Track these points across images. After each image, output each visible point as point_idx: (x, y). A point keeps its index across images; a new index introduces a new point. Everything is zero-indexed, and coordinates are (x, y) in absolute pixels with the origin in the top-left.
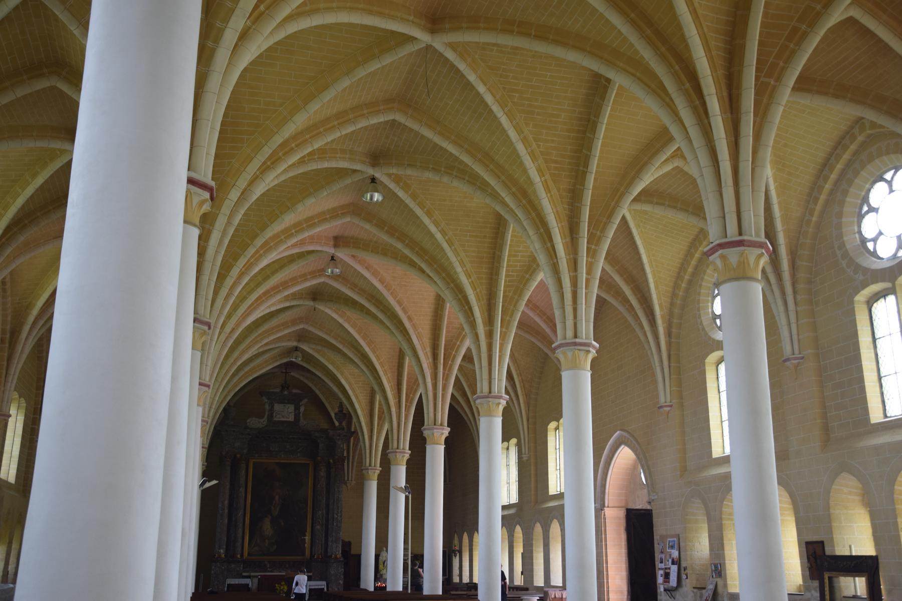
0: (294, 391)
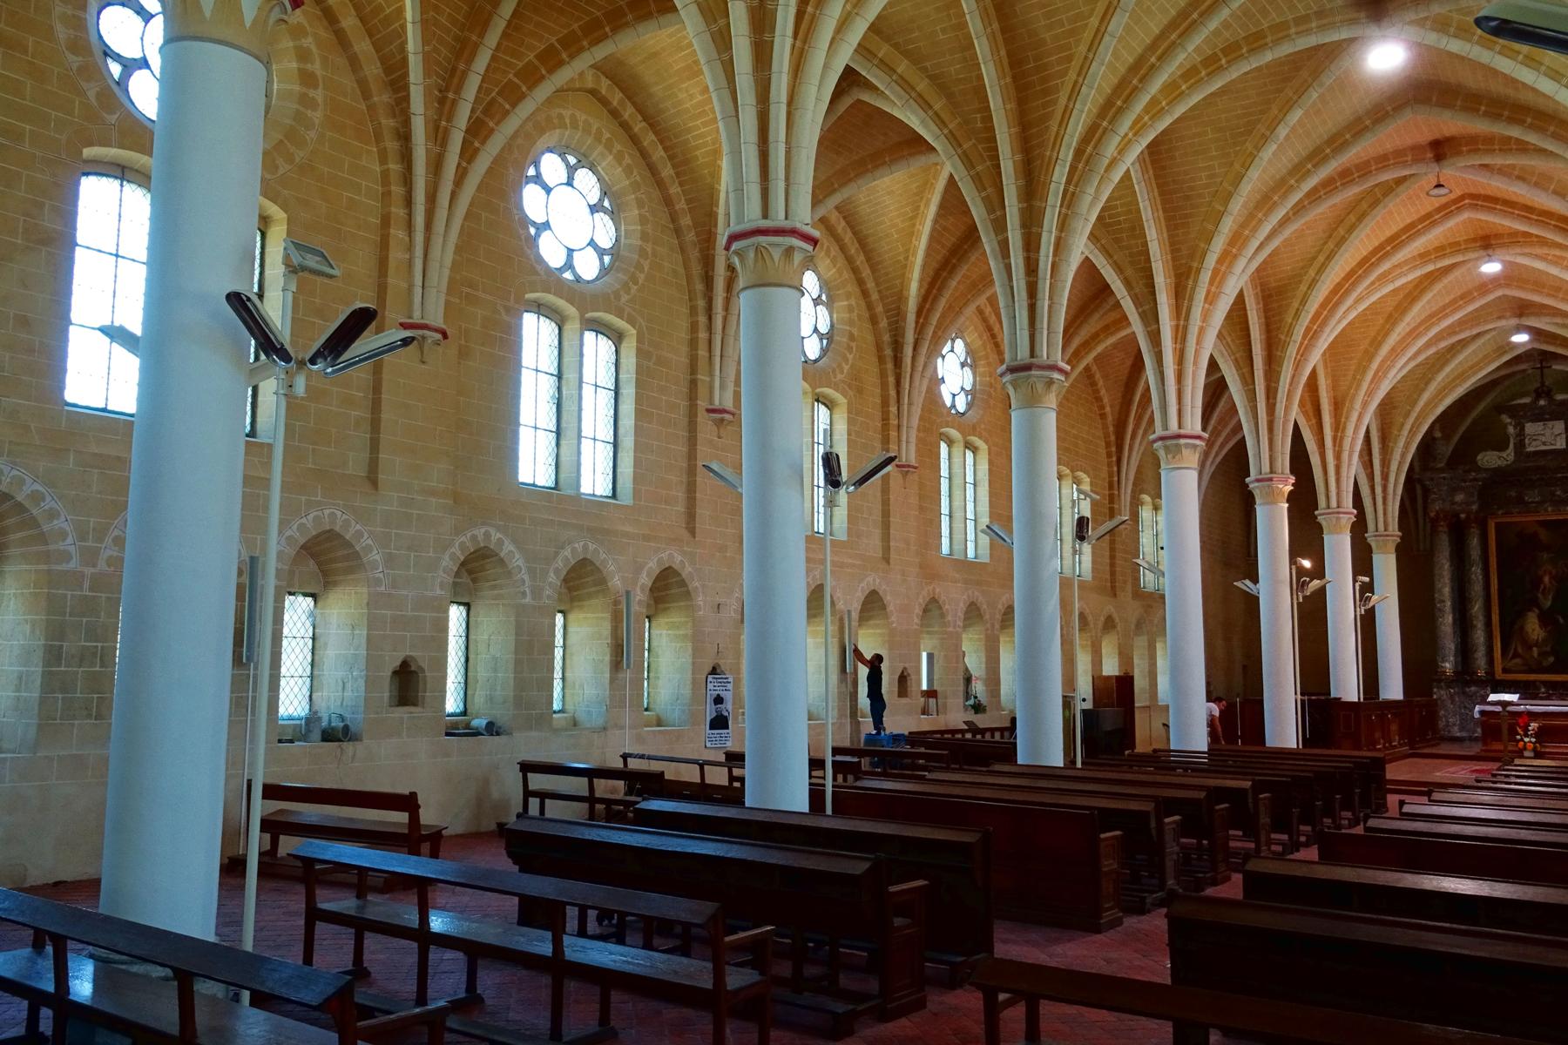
0: (1560, 397)
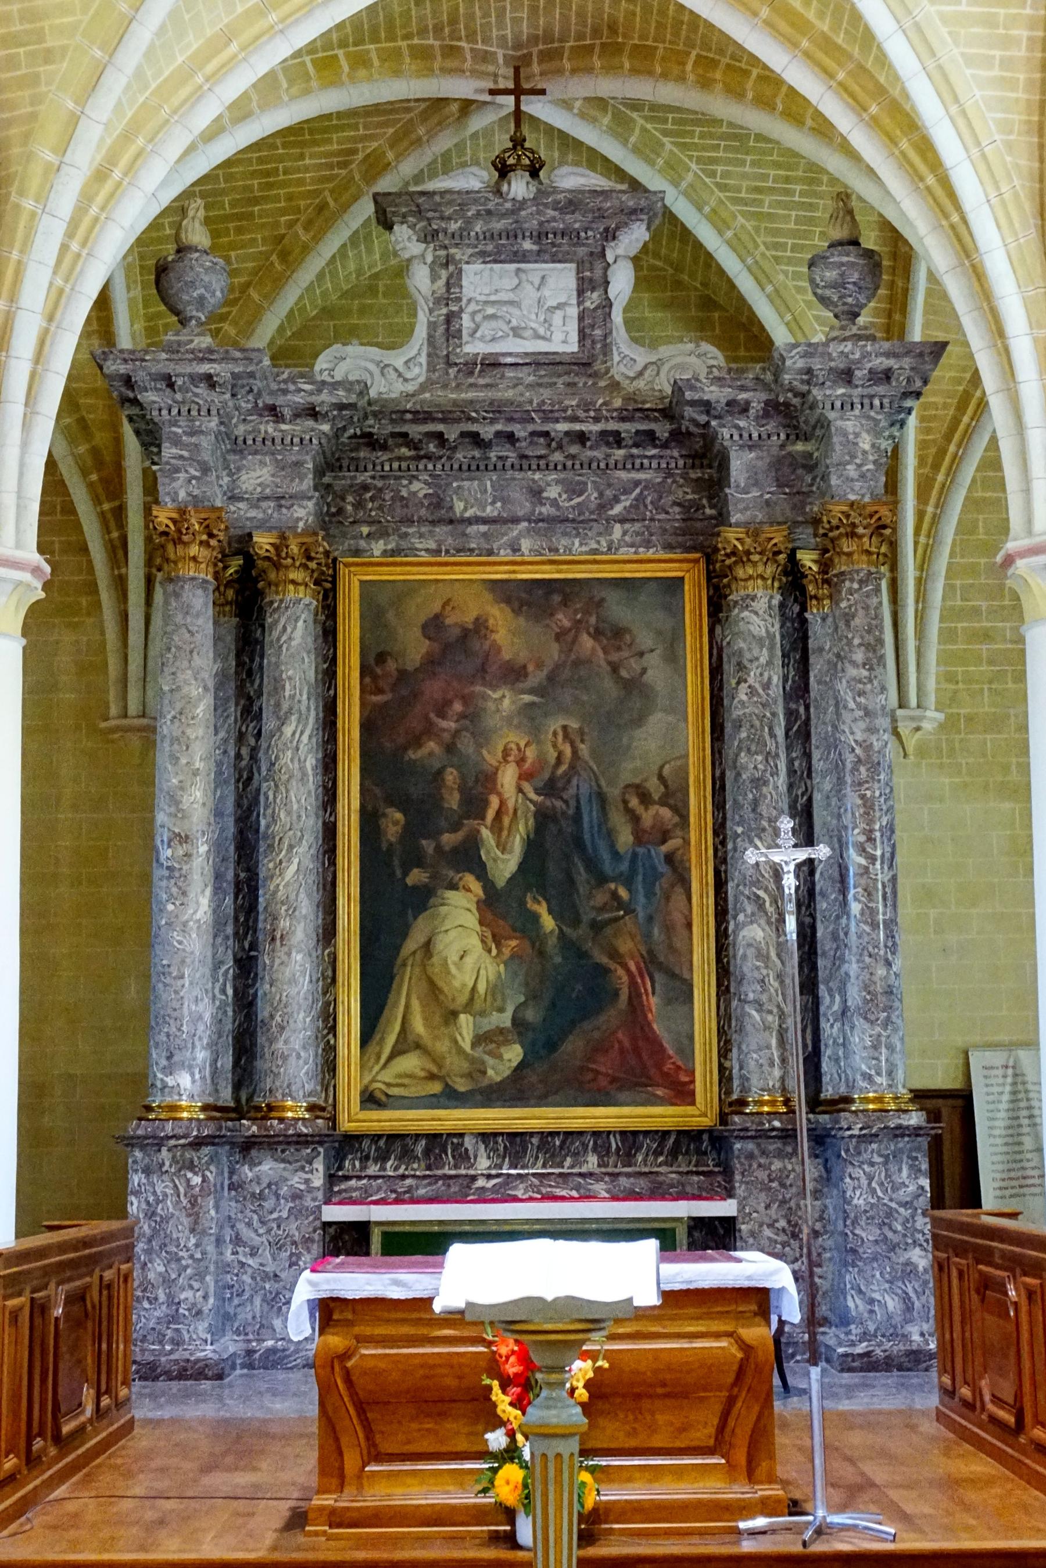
0: (570, 178)
